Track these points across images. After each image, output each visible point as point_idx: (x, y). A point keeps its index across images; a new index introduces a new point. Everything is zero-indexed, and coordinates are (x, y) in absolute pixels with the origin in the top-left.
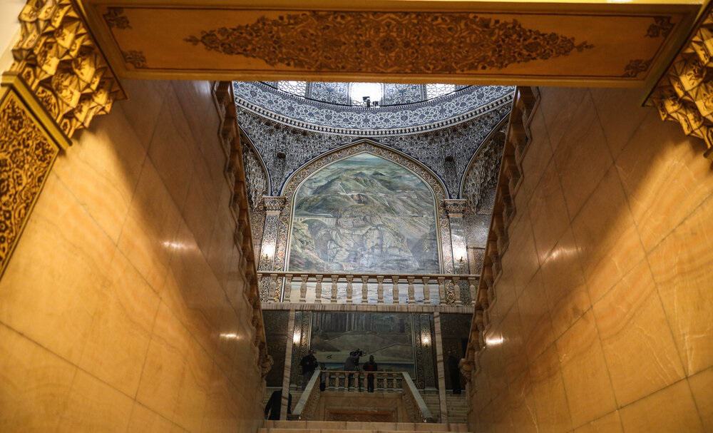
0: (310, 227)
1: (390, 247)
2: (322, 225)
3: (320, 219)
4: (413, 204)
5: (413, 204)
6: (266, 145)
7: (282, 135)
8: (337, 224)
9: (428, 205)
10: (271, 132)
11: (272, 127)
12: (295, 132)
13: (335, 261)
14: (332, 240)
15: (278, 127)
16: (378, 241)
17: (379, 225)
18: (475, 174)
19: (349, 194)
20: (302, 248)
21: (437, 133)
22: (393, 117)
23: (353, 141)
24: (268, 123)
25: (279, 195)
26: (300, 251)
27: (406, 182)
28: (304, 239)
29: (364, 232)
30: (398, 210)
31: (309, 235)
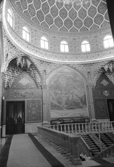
0: (55, 94)
2: (57, 93)
4: (79, 86)
5: (79, 86)
6: (41, 68)
8: (61, 93)
10: (41, 63)
16: (72, 98)
17: (72, 93)
20: (53, 101)
21: (86, 64)
22: (73, 57)
26: (53, 101)
27: (78, 79)
28: (53, 98)
29: (68, 95)
31: (54, 96)
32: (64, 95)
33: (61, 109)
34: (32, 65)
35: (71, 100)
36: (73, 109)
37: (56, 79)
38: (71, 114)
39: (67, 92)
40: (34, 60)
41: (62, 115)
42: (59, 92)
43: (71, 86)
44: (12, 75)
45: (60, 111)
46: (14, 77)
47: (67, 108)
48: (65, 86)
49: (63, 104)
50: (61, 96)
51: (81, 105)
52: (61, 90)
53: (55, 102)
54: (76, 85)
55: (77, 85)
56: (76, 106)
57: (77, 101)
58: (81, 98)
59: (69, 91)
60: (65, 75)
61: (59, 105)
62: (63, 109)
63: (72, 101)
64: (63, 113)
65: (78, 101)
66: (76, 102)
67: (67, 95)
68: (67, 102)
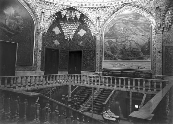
1: (134, 48)
2: (112, 42)
3: (112, 40)
5: (142, 30)
7: (97, 10)
9: (148, 30)
11: (94, 8)
12: (101, 8)
13: (116, 54)
14: (115, 47)
15: (95, 8)
17: (130, 40)
18: (169, 13)
19: (120, 29)
20: (107, 50)
23: (121, 6)
24: (92, 8)
25: (99, 33)
26: (106, 51)
27: (140, 21)
29: (125, 43)
30: (137, 33)
32: (120, 44)
33: (115, 60)
34: (82, 15)
35: (128, 49)
36: (130, 60)
37: (112, 26)
38: (126, 66)
39: (124, 40)
40: (82, 10)
41: (115, 66)
42: (114, 40)
43: (129, 31)
44: (71, 28)
45: (113, 62)
46: (73, 29)
47: (121, 59)
48: (122, 32)
49: (117, 53)
50: (116, 45)
51: (142, 55)
52: (117, 38)
53: (108, 51)
54: (137, 30)
55: (138, 29)
56: (134, 56)
57: (136, 50)
58: (143, 46)
59: (126, 38)
60: (123, 19)
61: (112, 55)
62: (117, 60)
63: (129, 50)
64: (116, 64)
65: (138, 50)
66: (134, 51)
67: (123, 44)
68: (123, 51)
